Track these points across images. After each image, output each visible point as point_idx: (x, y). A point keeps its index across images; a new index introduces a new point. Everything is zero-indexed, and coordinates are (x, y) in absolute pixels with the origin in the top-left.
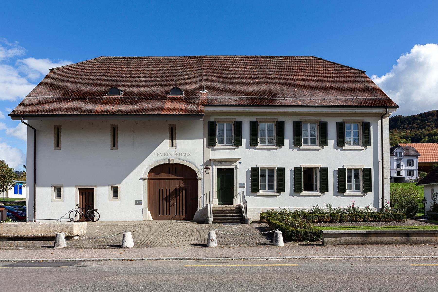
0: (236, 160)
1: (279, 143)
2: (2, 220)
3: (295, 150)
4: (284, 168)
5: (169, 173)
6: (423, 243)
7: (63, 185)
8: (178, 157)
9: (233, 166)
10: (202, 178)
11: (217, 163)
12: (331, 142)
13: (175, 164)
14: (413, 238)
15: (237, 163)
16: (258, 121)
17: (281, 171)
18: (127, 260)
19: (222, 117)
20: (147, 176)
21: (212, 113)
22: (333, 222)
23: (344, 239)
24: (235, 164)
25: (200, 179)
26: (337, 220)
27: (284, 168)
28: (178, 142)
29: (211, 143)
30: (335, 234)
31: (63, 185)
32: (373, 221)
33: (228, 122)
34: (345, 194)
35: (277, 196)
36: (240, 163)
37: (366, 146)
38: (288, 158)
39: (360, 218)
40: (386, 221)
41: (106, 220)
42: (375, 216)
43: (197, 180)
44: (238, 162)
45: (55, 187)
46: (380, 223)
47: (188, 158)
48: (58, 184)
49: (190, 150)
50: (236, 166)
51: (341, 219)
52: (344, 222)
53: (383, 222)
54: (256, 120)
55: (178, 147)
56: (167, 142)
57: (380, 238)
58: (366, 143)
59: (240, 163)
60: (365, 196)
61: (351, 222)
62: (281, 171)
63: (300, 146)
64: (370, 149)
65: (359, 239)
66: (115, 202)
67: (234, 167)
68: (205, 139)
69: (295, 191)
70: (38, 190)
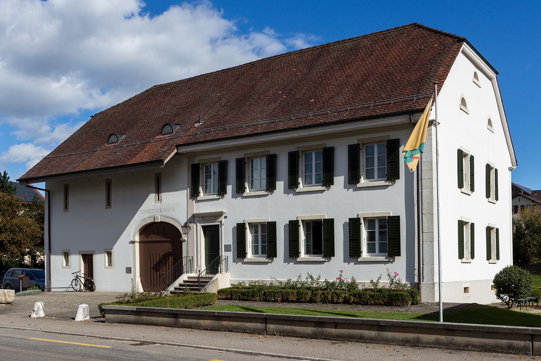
0: (220, 214)
1: (269, 187)
2: (1, 288)
3: (291, 195)
4: (333, 220)
5: (158, 235)
6: (190, 327)
7: (94, 251)
8: (162, 214)
9: (218, 222)
10: (186, 239)
11: (201, 219)
12: (340, 180)
13: (162, 223)
14: (181, 320)
15: (222, 219)
16: (300, 150)
17: (271, 227)
18: (96, 337)
19: (207, 157)
20: (137, 239)
21: (194, 154)
22: (301, 302)
23: (120, 316)
24: (220, 220)
25: (184, 241)
26: (305, 299)
27: (333, 220)
28: (163, 195)
29: (194, 194)
30: (114, 310)
31: (94, 251)
32: (356, 303)
33: (379, 142)
34: (359, 260)
35: (268, 262)
36: (226, 217)
37: (394, 180)
38: (283, 207)
39: (338, 298)
40: (376, 304)
41: (103, 291)
42: (360, 295)
43: (181, 243)
44: (223, 217)
45: (82, 255)
46: (366, 307)
47: (171, 214)
48: (87, 250)
49: (172, 205)
50: (221, 222)
51: (311, 298)
52: (316, 302)
53: (371, 304)
54: (356, 143)
55: (162, 201)
56: (152, 196)
57: (151, 318)
58: (392, 175)
59: (226, 217)
60: (392, 262)
61: (326, 303)
62: (271, 227)
63: (356, 184)
64: (401, 183)
65: (132, 317)
66: (110, 270)
67: (219, 223)
68: (189, 189)
69: (350, 256)
70: (53, 257)
